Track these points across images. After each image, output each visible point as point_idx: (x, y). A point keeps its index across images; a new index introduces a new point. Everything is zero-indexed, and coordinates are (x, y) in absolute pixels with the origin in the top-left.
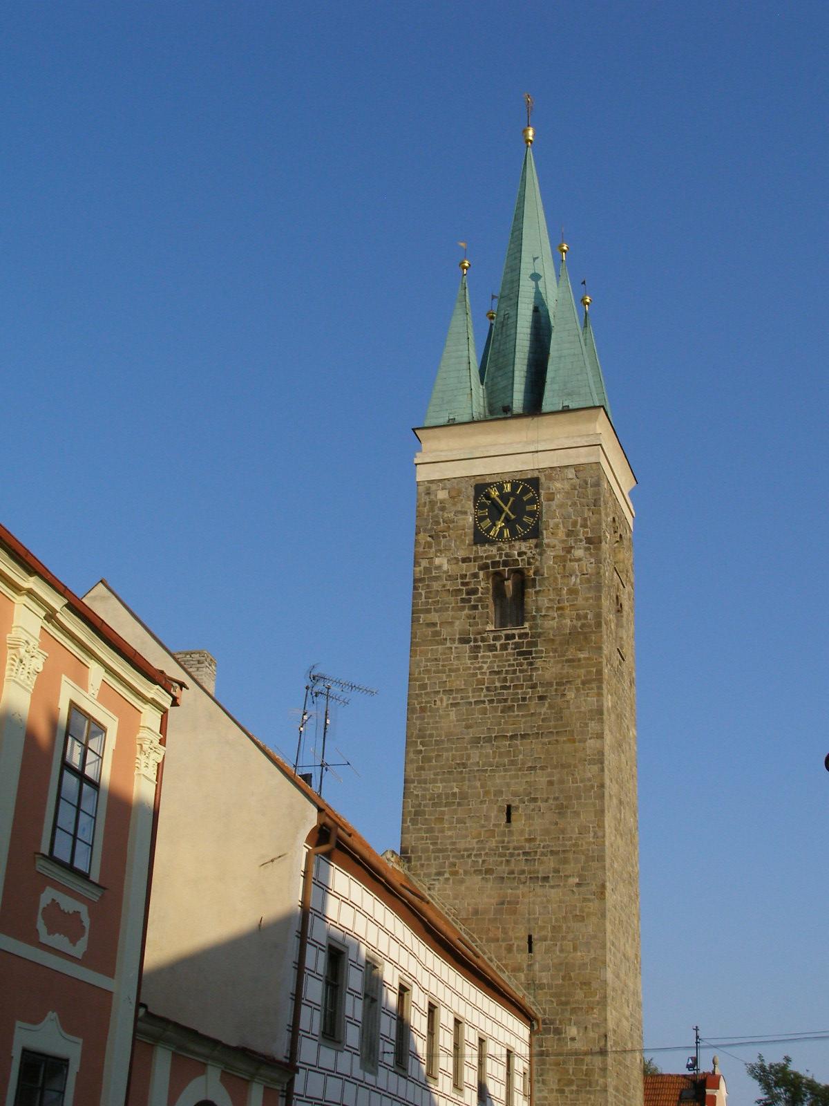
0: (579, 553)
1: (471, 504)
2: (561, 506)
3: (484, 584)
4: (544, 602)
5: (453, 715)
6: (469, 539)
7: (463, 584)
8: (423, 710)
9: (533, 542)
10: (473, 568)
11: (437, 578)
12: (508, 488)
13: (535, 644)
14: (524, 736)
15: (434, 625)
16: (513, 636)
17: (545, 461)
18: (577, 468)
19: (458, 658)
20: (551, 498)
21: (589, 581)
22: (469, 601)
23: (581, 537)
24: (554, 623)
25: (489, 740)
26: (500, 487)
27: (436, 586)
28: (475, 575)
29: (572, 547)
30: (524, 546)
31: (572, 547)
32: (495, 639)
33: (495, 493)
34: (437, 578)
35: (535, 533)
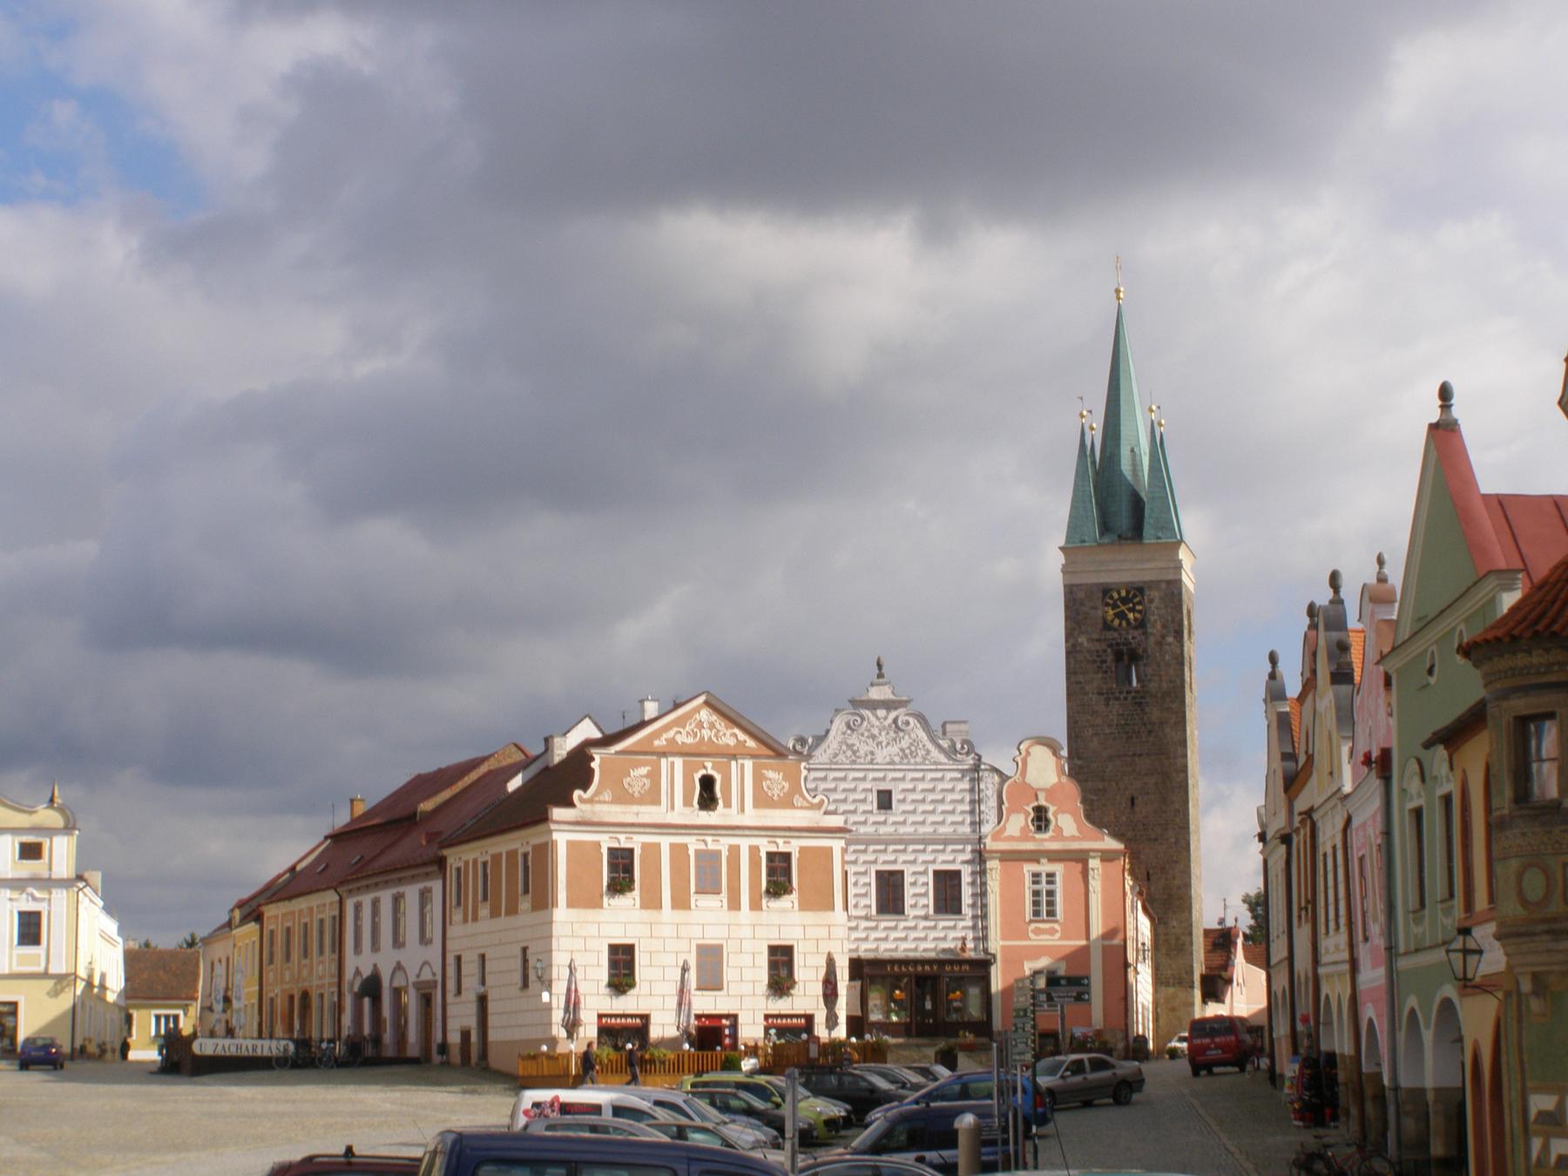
3: (1110, 658)
4: (1149, 671)
5: (1095, 740)
6: (1100, 626)
10: (1104, 646)
12: (1123, 593)
17: (1147, 577)
18: (1169, 582)
20: (1151, 601)
30: (1136, 633)
33: (1116, 595)
35: (1141, 624)
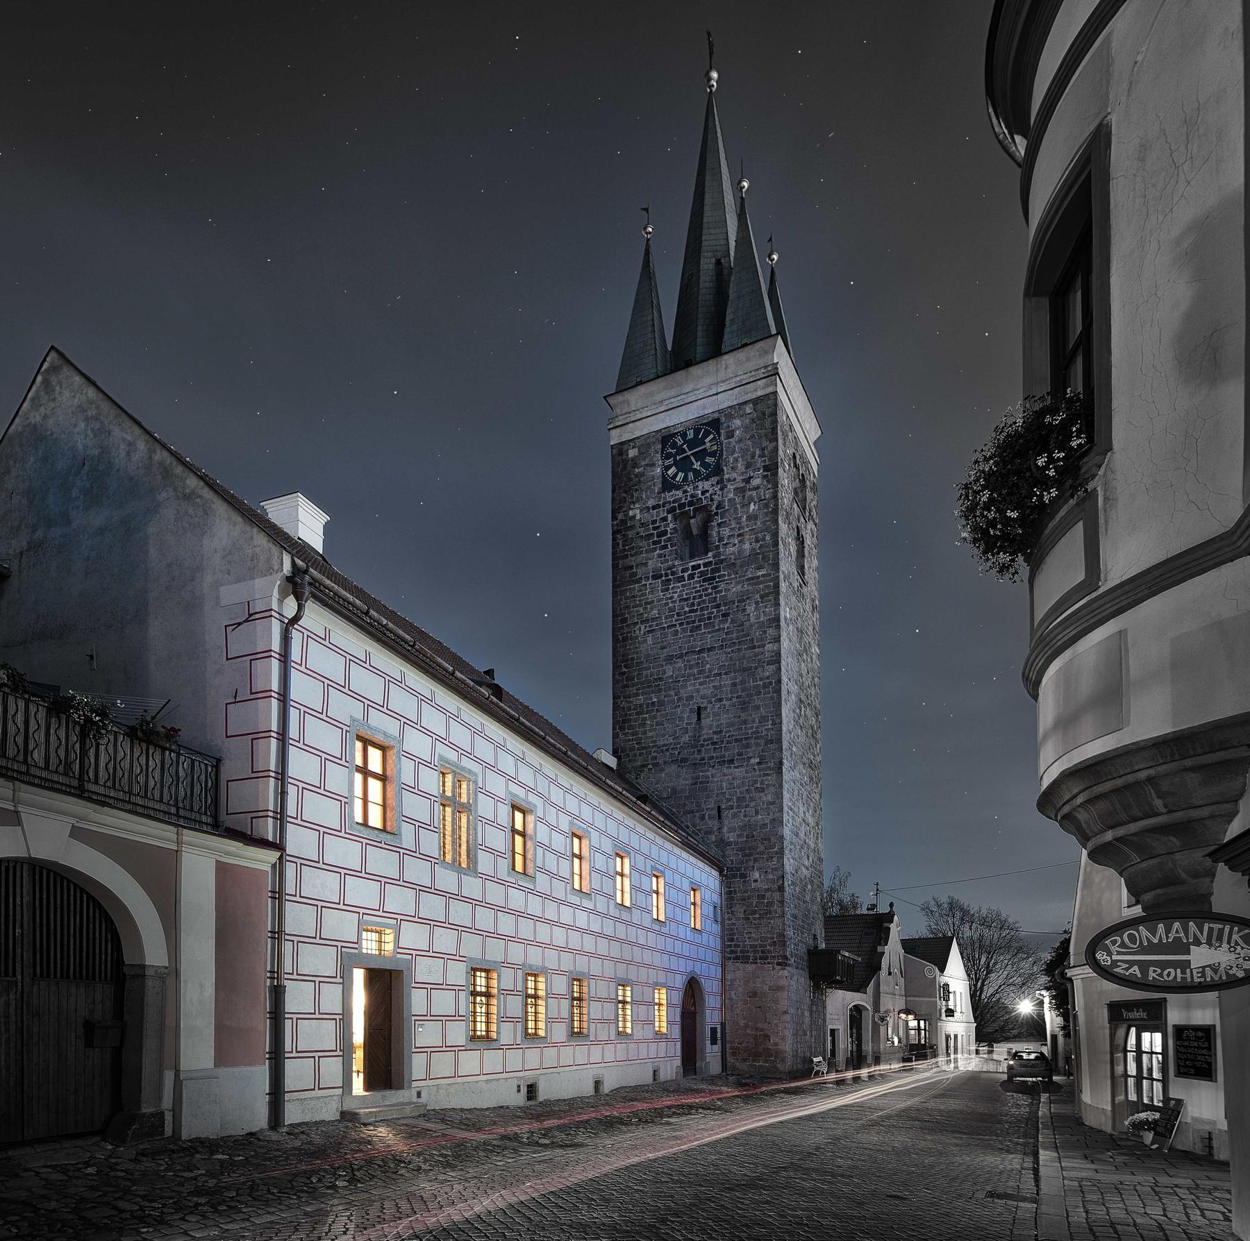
0: (756, 482)
1: (659, 455)
2: (740, 441)
7: (654, 529)
8: (625, 639)
9: (714, 479)
11: (632, 527)
12: (690, 434)
13: (718, 570)
14: (709, 650)
15: (631, 567)
16: (699, 566)
18: (756, 402)
19: (652, 592)
20: (730, 435)
21: (767, 506)
22: (660, 542)
23: (758, 465)
24: (735, 549)
25: (681, 656)
26: (684, 435)
27: (630, 534)
28: (665, 519)
29: (751, 477)
30: (707, 485)
31: (751, 477)
32: (683, 571)
34: (632, 527)
